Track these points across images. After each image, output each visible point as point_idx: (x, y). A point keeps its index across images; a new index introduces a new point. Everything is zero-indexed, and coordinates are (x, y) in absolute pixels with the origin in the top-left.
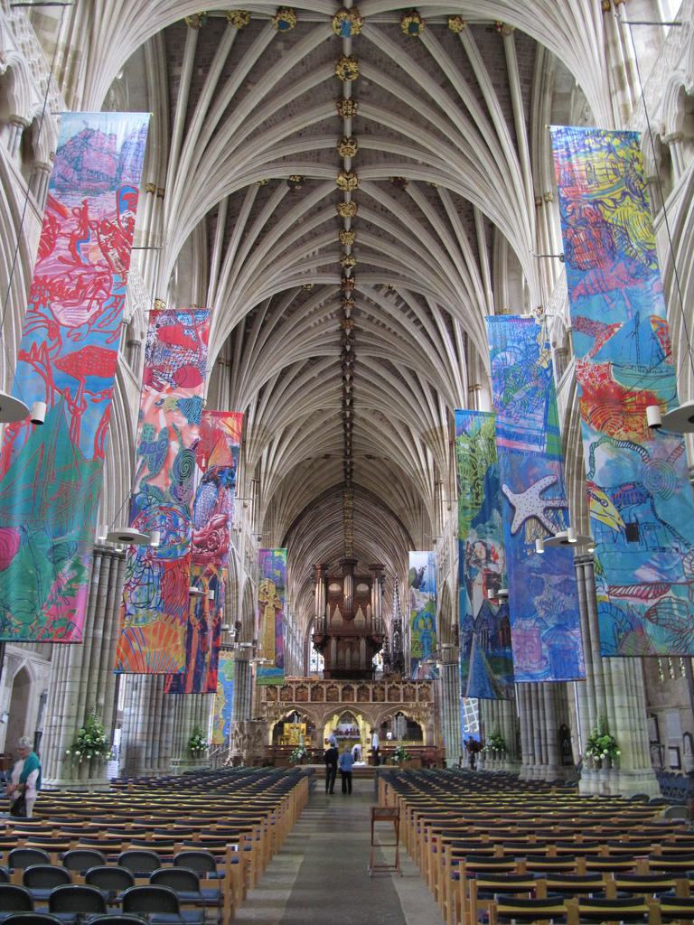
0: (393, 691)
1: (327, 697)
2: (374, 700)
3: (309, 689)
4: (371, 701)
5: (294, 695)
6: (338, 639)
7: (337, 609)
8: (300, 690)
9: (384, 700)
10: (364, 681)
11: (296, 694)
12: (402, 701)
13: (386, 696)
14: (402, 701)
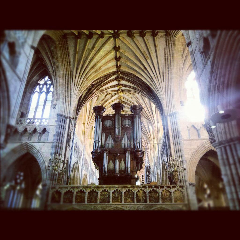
0: (153, 194)
1: (100, 199)
2: (137, 202)
3: (87, 194)
4: (136, 203)
5: (74, 198)
6: (110, 153)
7: (110, 136)
8: (79, 194)
9: (146, 201)
10: (129, 186)
11: (76, 198)
12: (161, 202)
13: (148, 198)
14: (161, 202)
